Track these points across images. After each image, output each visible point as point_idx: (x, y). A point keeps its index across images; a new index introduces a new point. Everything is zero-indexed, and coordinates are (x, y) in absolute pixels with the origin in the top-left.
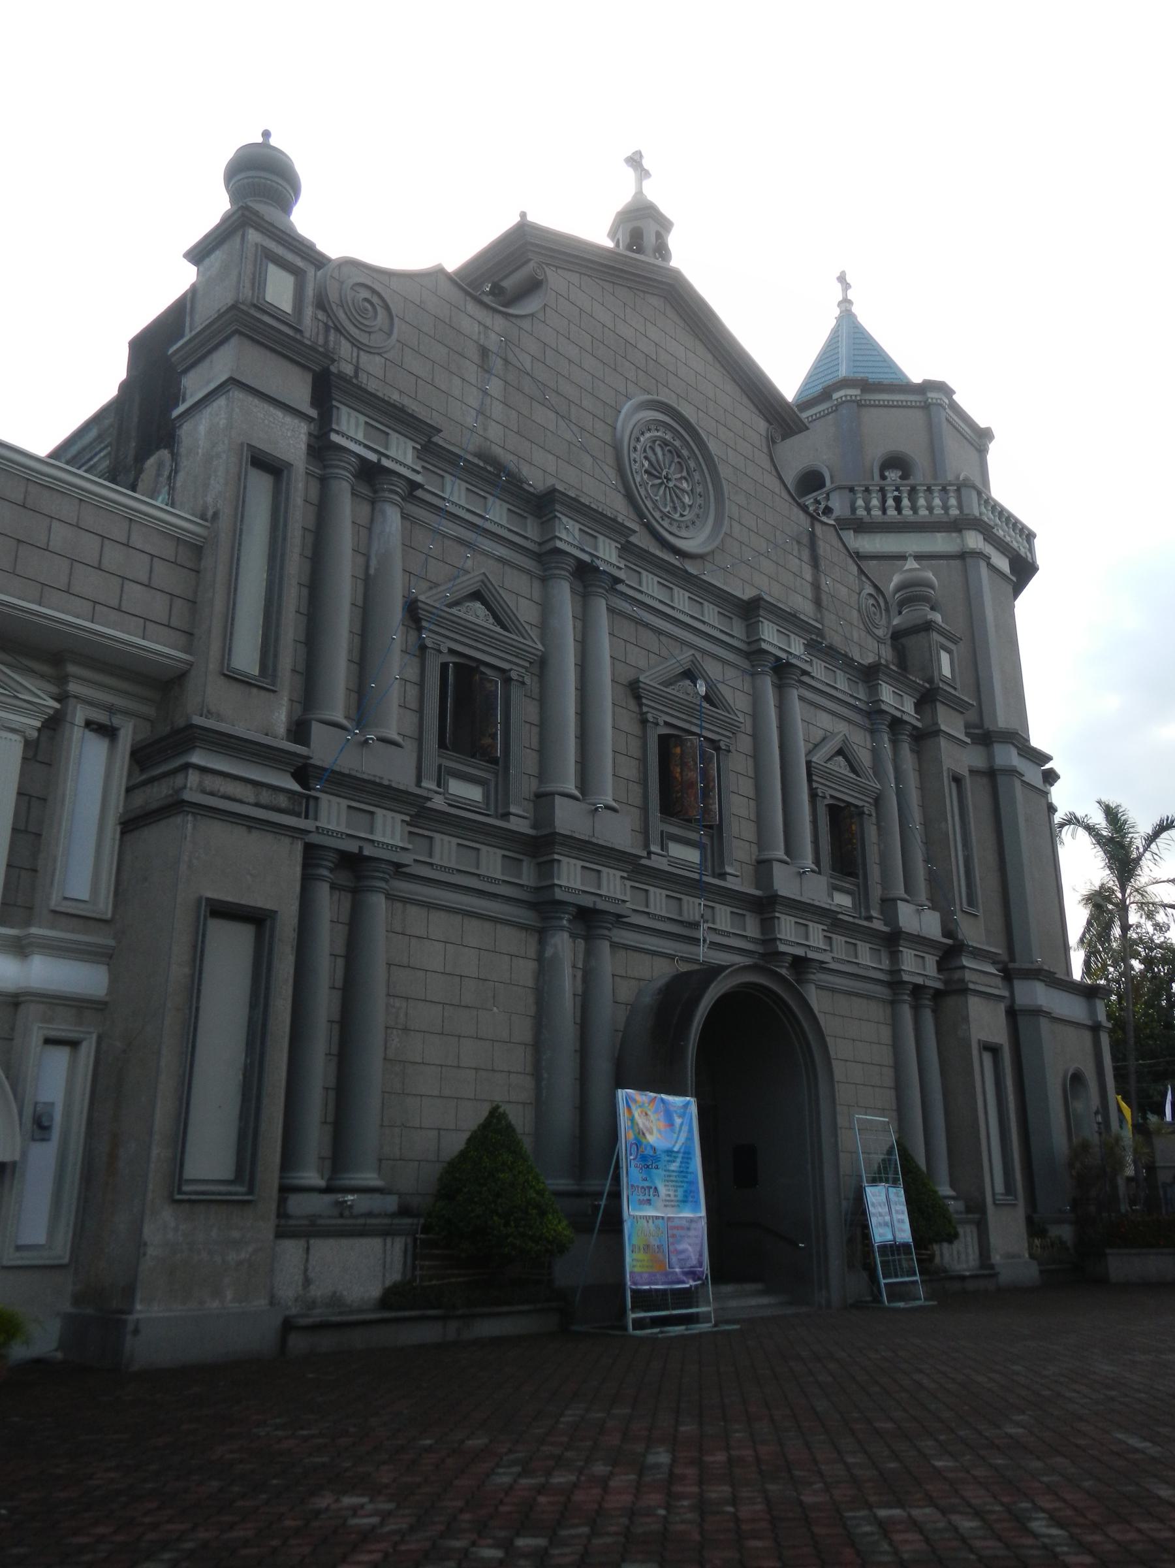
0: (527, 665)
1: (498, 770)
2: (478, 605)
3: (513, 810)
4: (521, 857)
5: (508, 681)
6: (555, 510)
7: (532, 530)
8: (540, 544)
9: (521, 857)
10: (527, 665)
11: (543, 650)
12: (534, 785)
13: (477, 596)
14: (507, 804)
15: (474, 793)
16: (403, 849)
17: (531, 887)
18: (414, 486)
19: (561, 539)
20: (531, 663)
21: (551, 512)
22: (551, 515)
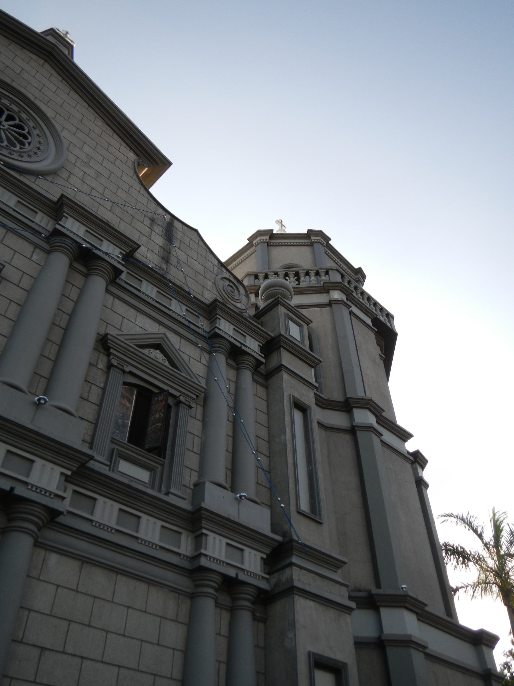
0: (195, 397)
1: (164, 462)
2: (158, 351)
3: (172, 490)
4: (180, 530)
5: (179, 403)
6: (217, 314)
7: (203, 324)
8: (208, 333)
9: (180, 530)
10: (195, 397)
11: (206, 388)
12: (194, 477)
13: (158, 347)
14: (169, 486)
15: (144, 475)
16: (57, 495)
17: (187, 557)
18: (118, 272)
19: (220, 329)
20: (197, 396)
21: (214, 316)
22: (215, 317)
